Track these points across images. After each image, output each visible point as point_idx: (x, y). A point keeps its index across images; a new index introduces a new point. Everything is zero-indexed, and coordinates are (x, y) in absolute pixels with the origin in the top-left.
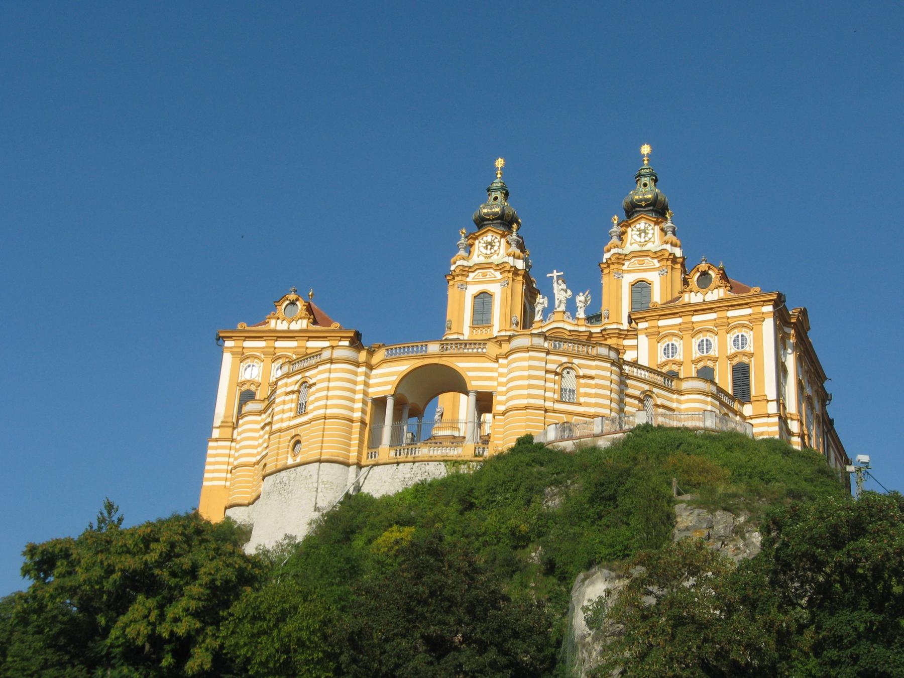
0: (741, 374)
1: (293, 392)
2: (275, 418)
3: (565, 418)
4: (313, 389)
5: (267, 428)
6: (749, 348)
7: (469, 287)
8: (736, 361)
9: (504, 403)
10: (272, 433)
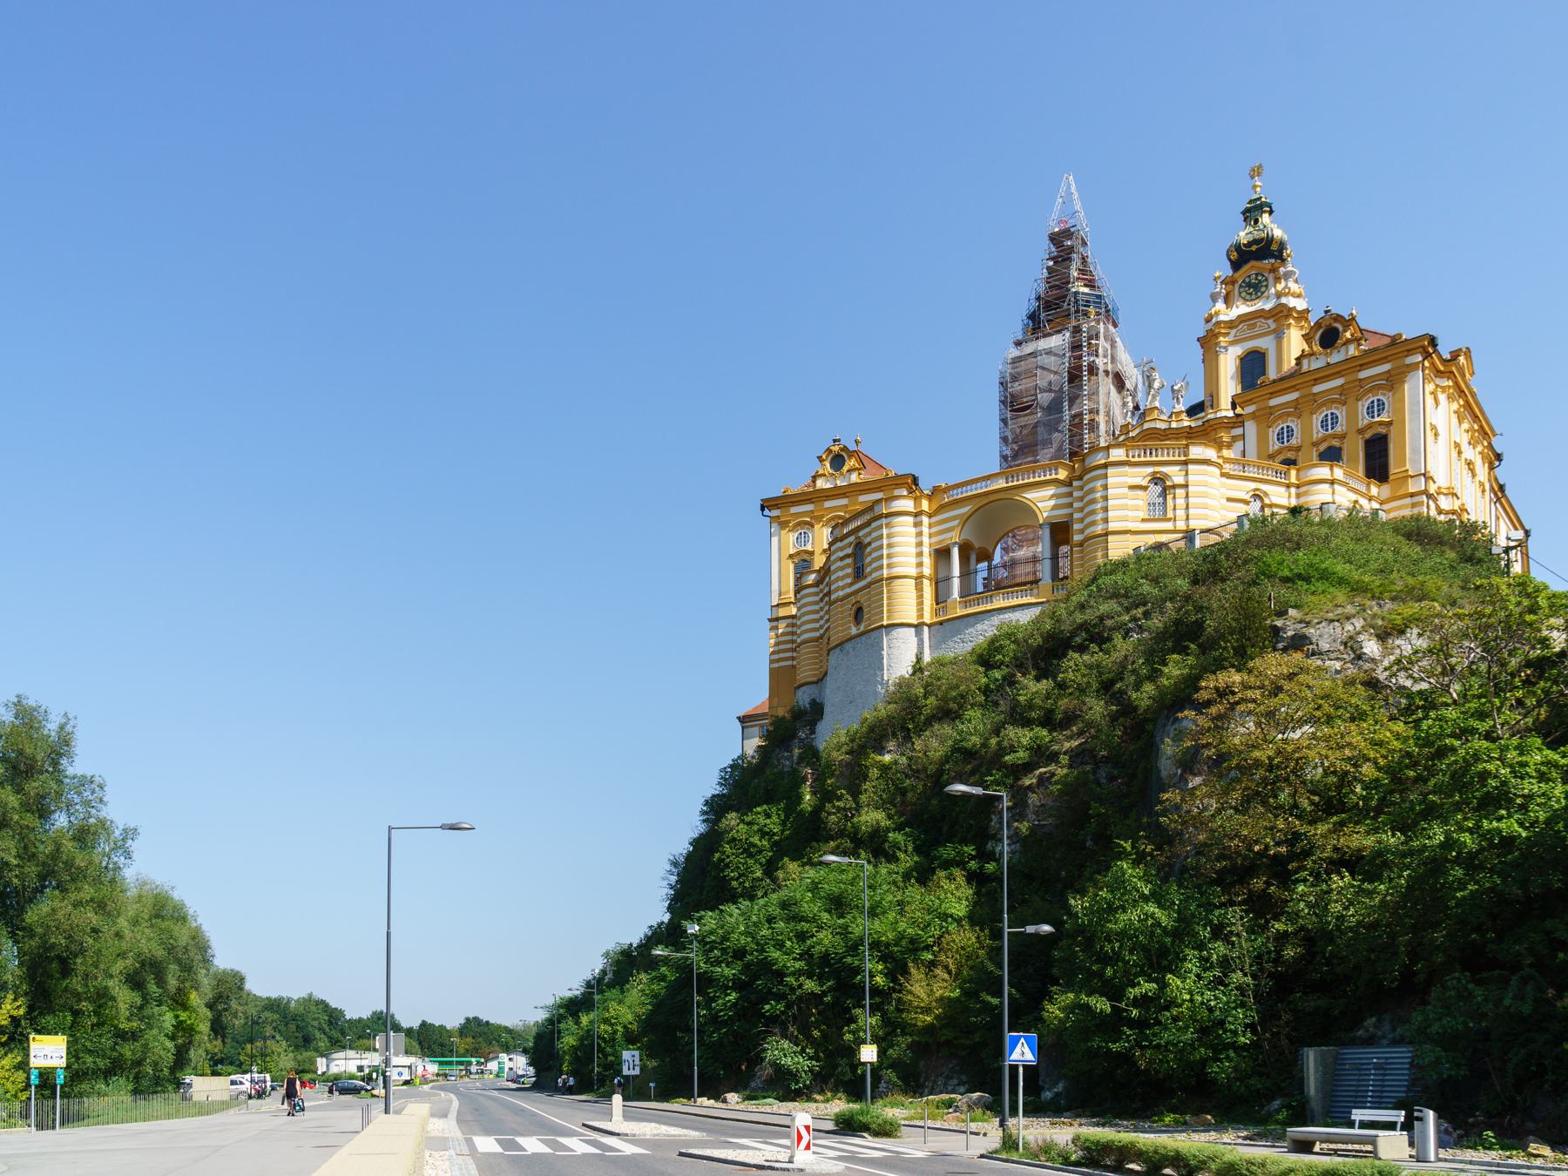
1: (847, 556)
2: (833, 588)
4: (868, 549)
5: (827, 599)
8: (1368, 435)
9: (1082, 531)
10: (831, 603)
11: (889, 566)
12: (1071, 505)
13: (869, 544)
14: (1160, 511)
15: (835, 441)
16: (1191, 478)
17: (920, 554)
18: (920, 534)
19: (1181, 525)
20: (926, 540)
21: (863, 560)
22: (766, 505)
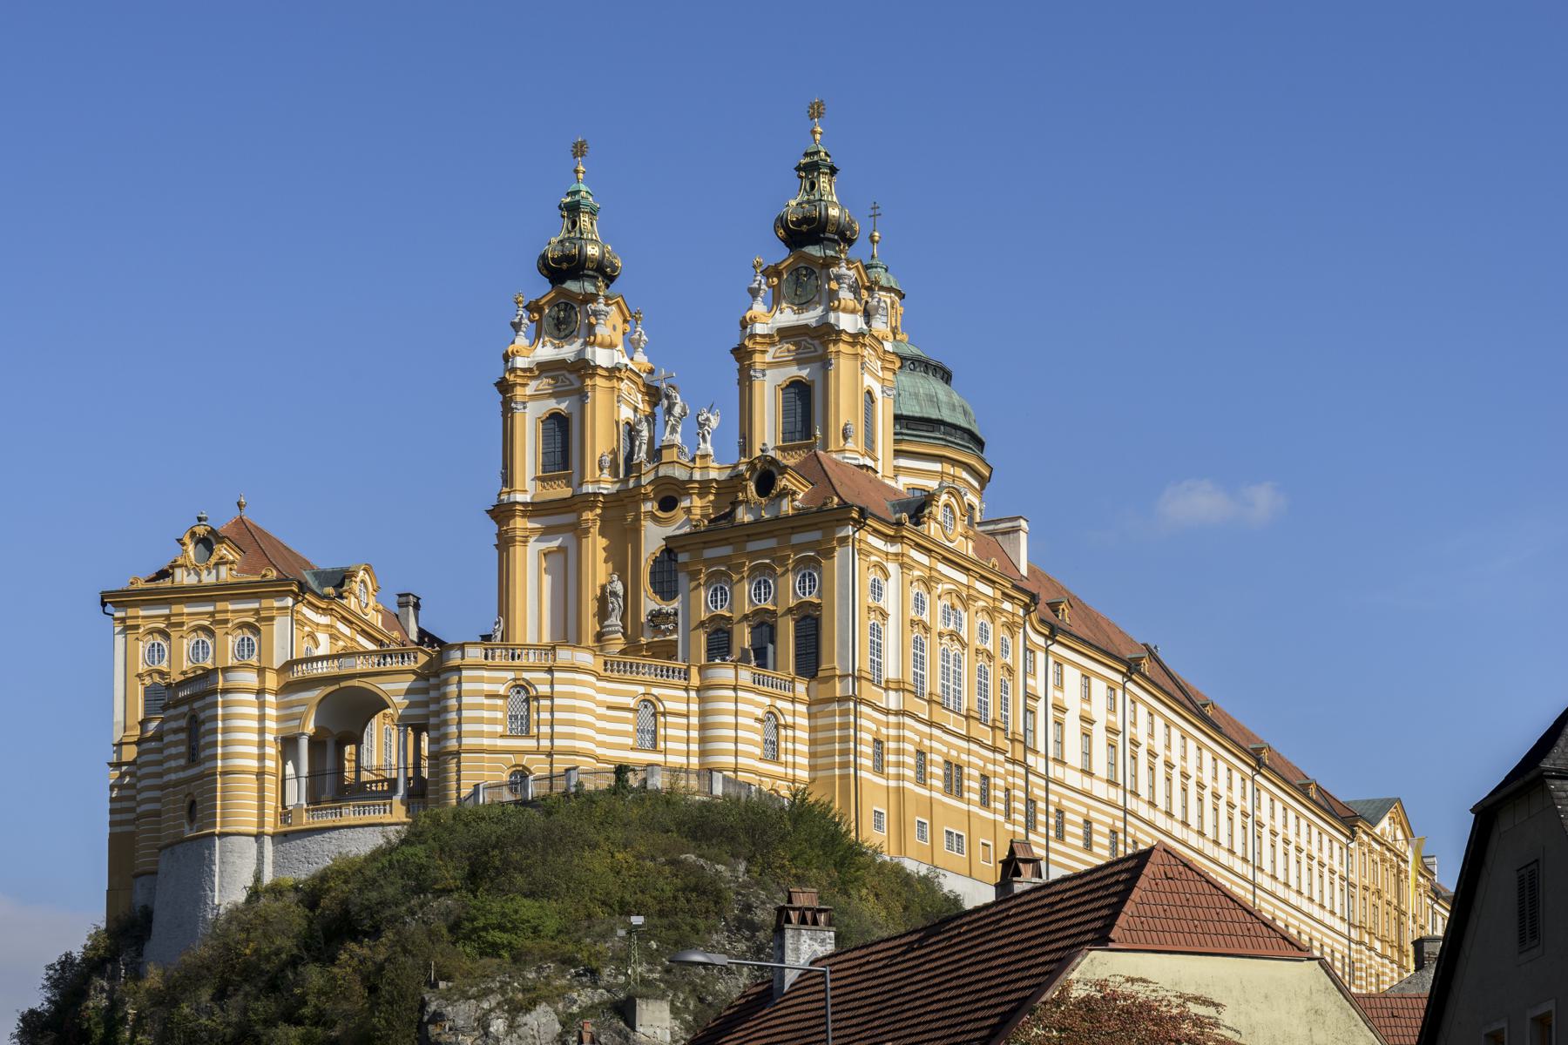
3: (513, 759)
11: (225, 757)
12: (426, 704)
13: (203, 722)
14: (522, 725)
15: (200, 519)
16: (557, 688)
17: (262, 744)
18: (262, 718)
20: (271, 725)
21: (197, 741)
22: (106, 599)
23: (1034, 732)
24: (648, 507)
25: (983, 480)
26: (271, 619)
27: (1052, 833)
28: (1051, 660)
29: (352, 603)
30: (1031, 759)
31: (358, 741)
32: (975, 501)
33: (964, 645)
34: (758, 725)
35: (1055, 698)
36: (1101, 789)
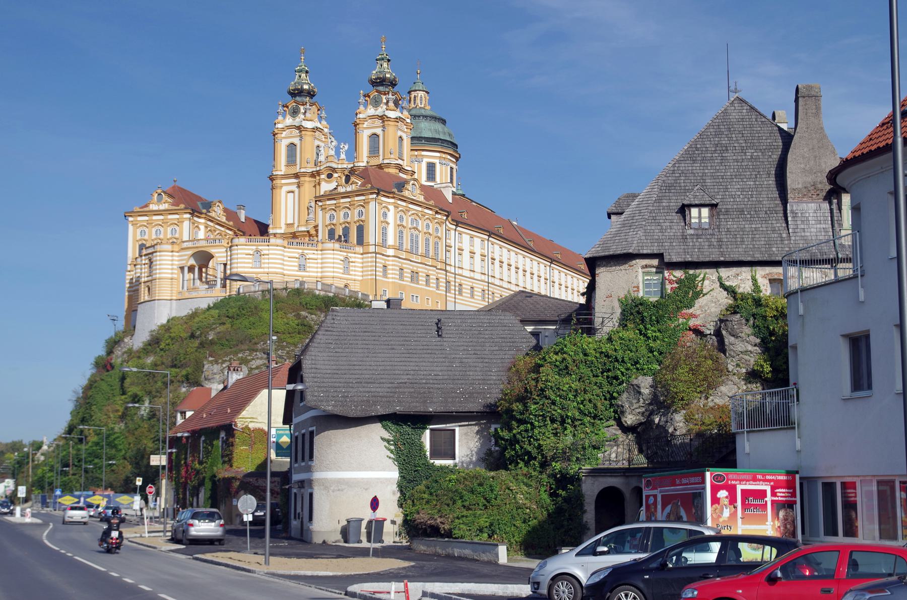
0: (361, 230)
6: (363, 218)
7: (283, 140)
19: (266, 270)
23: (450, 258)
24: (323, 176)
25: (457, 159)
26: (183, 222)
27: (457, 293)
28: (457, 233)
29: (213, 214)
30: (448, 268)
31: (207, 267)
32: (454, 166)
33: (420, 232)
34: (342, 262)
35: (459, 246)
36: (478, 276)
